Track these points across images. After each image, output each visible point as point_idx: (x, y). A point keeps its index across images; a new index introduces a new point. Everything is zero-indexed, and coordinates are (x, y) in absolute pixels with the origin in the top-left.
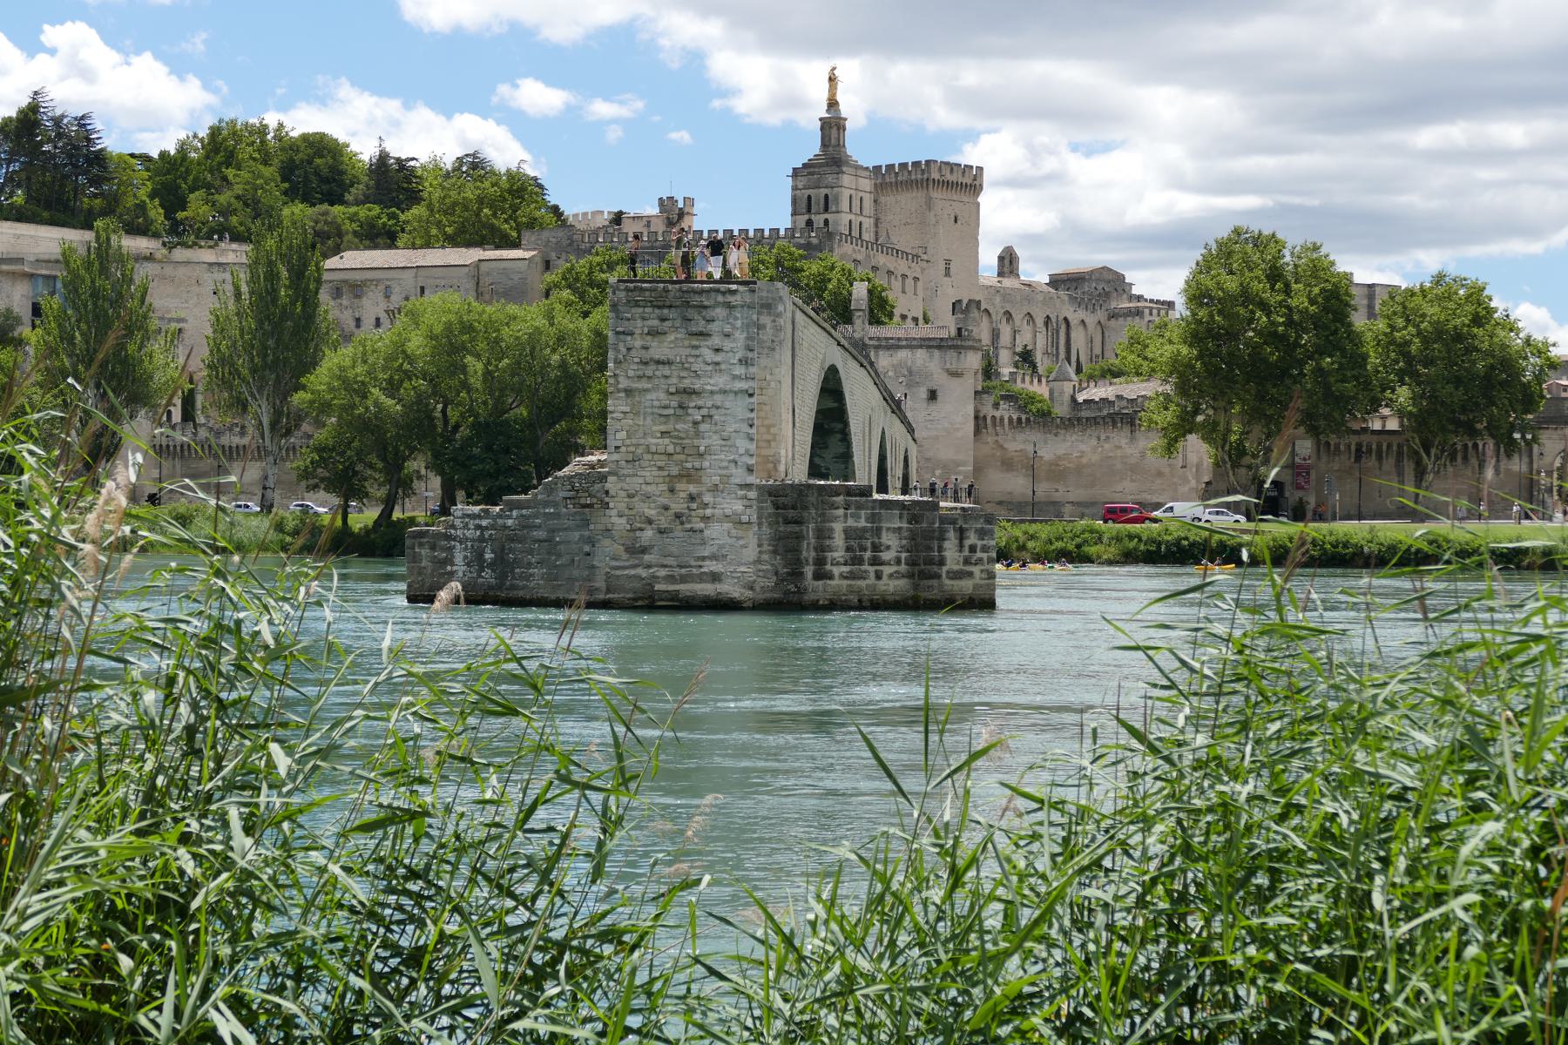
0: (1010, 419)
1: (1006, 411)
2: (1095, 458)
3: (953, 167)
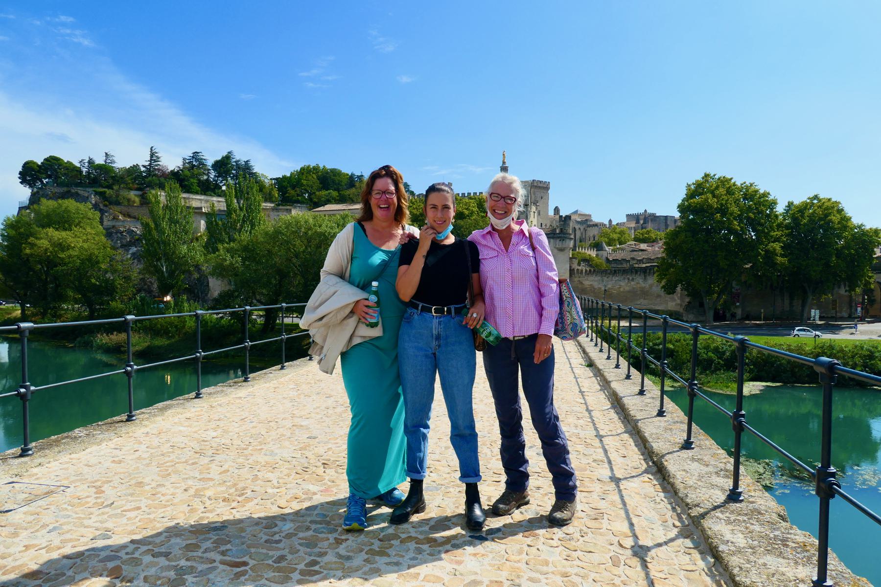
0: (586, 271)
1: (583, 267)
2: (627, 288)
3: (541, 182)
